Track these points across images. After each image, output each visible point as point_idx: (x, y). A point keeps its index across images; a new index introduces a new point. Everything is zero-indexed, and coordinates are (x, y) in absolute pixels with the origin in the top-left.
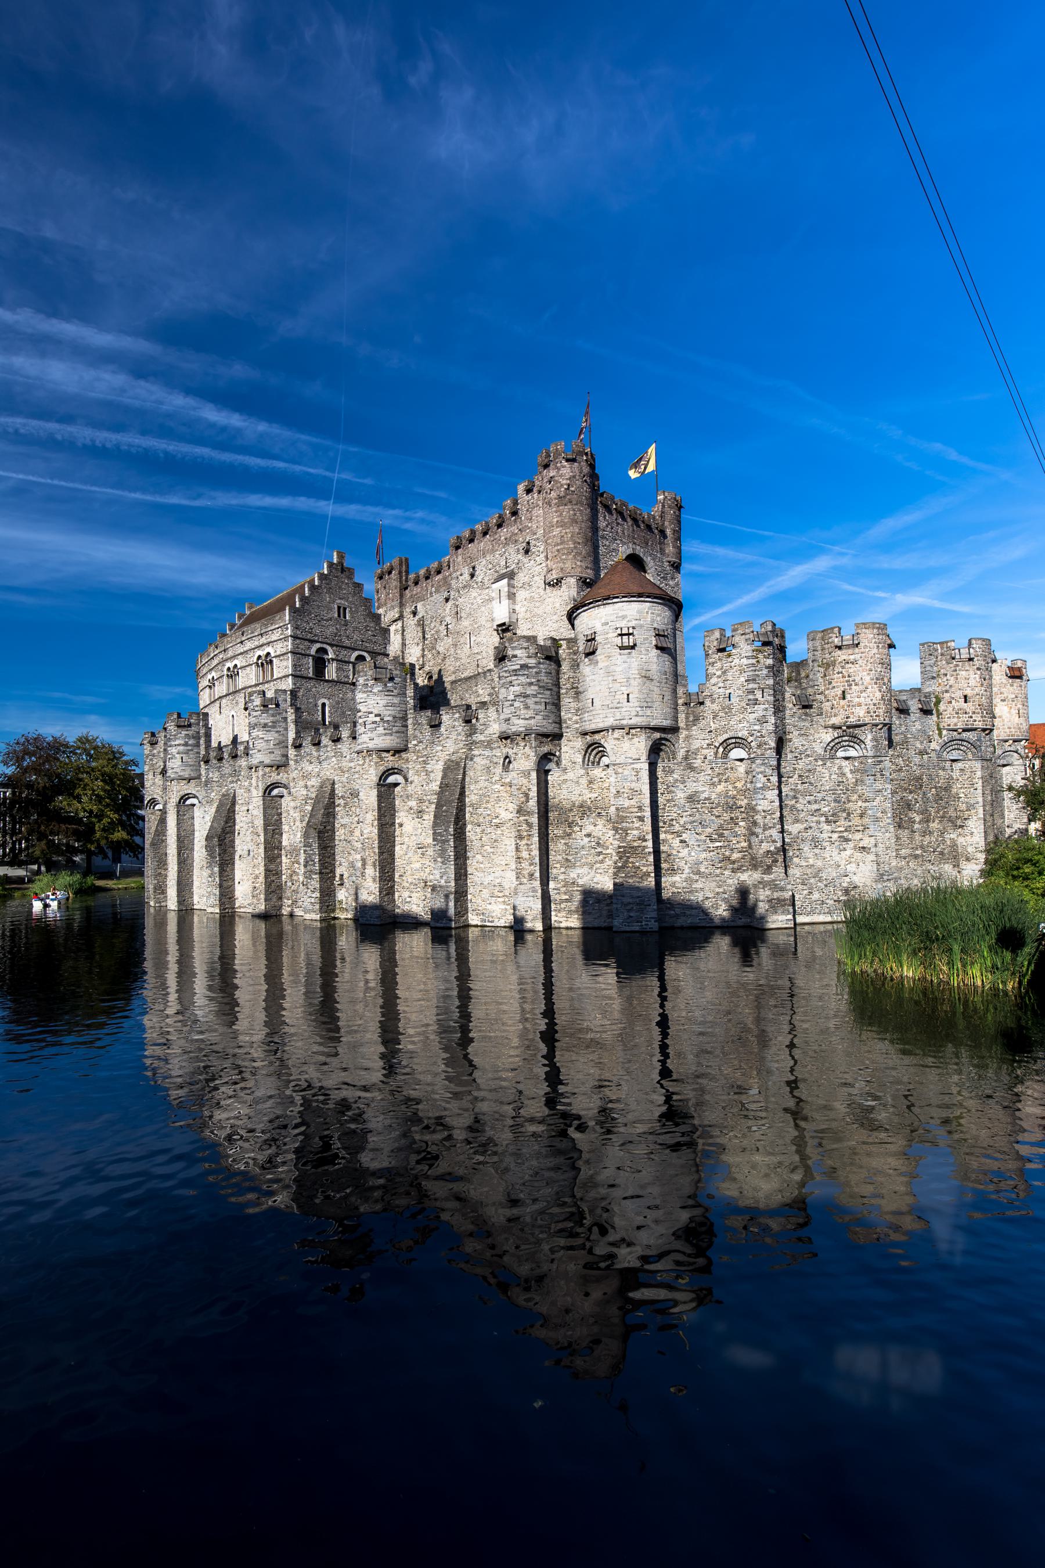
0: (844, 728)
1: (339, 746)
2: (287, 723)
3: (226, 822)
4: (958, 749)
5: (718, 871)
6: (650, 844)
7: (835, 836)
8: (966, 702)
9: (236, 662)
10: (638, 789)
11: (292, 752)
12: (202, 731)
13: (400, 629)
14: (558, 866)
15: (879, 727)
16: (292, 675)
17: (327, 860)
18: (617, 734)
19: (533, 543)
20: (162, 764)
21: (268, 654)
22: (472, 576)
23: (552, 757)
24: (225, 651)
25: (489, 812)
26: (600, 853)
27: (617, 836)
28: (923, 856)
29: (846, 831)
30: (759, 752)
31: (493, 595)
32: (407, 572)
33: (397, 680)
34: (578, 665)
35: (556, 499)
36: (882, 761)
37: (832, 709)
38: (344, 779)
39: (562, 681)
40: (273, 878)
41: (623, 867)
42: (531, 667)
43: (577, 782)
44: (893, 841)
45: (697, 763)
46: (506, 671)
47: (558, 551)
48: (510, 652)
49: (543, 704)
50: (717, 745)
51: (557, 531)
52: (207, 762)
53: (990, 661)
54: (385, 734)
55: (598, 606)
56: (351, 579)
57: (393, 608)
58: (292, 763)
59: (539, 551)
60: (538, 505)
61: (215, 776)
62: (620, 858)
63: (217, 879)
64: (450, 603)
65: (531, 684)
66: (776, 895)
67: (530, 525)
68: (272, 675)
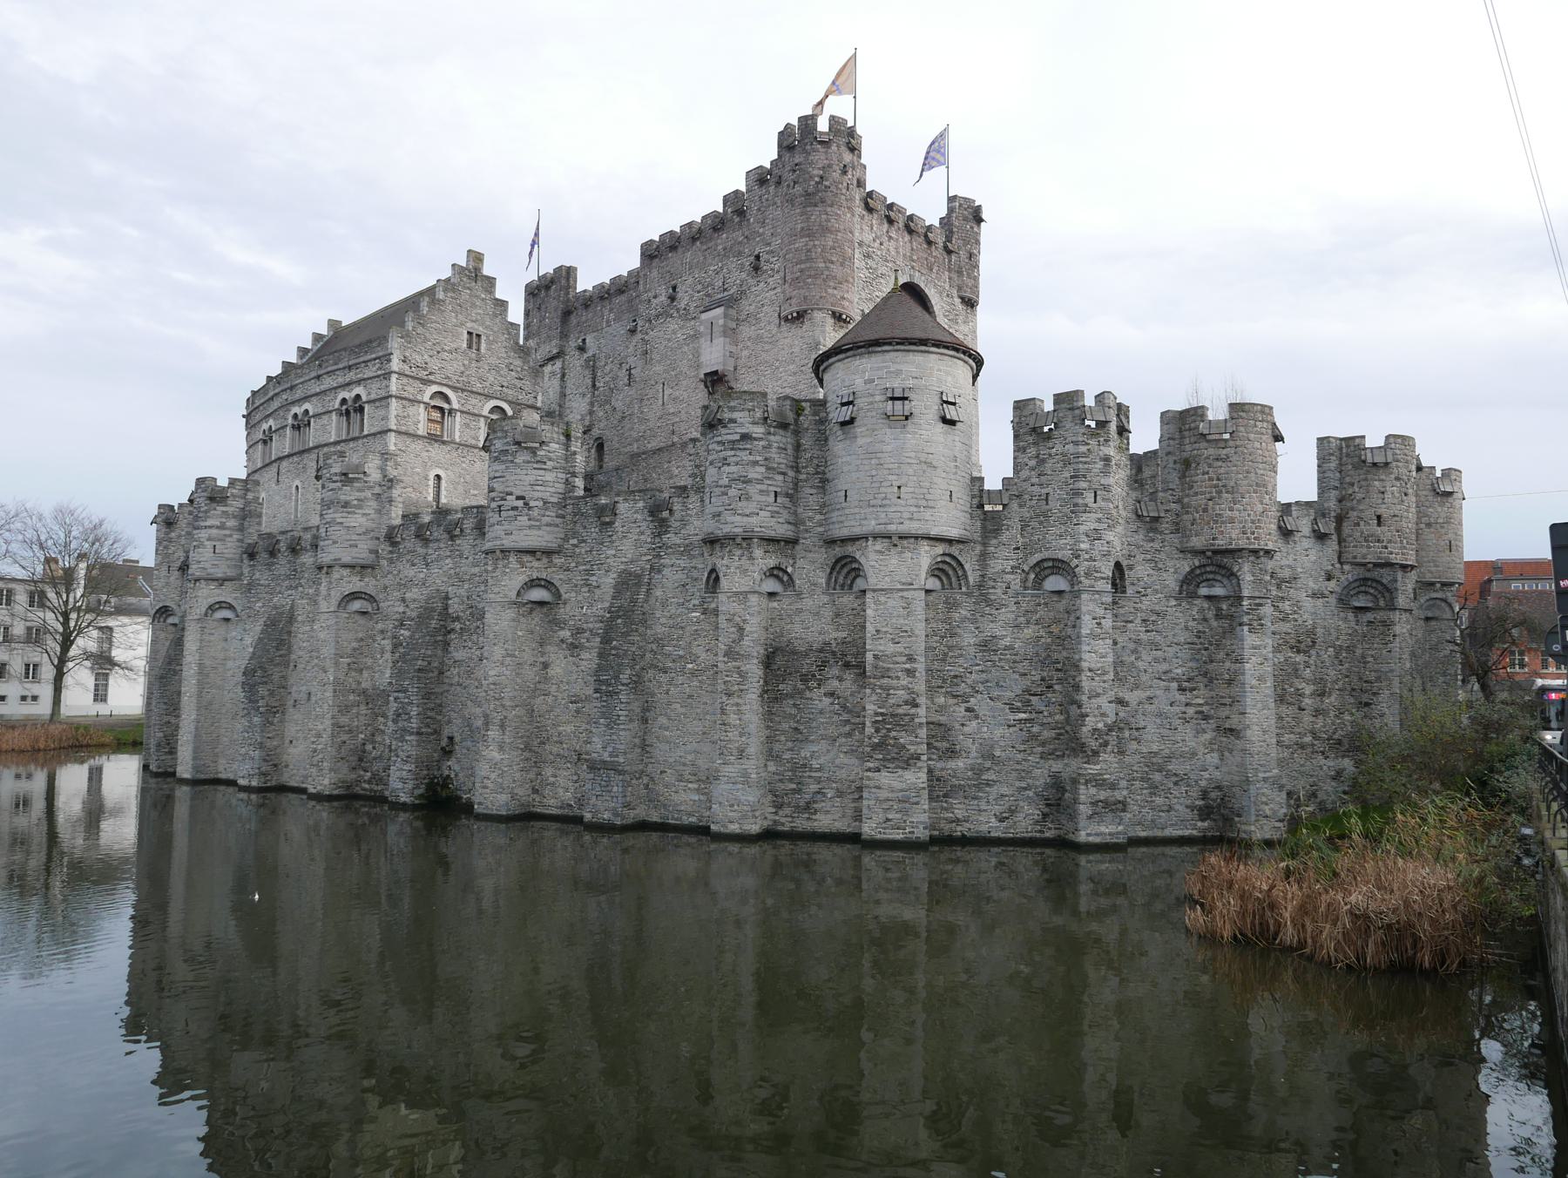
0: (1209, 554)
1: (458, 542)
4: (1366, 593)
5: (1020, 756)
6: (922, 711)
7: (1191, 711)
8: (1379, 524)
9: (307, 406)
10: (908, 628)
13: (558, 371)
14: (783, 738)
15: (1262, 553)
17: (429, 714)
18: (879, 545)
19: (764, 257)
20: (181, 554)
21: (358, 397)
22: (672, 299)
23: (781, 574)
24: (292, 388)
25: (681, 653)
26: (847, 722)
27: (874, 698)
28: (1313, 745)
29: (1207, 703)
30: (1086, 582)
31: (702, 329)
33: (554, 446)
34: (826, 440)
35: (803, 196)
36: (1261, 605)
37: (1193, 525)
38: (462, 592)
39: (802, 462)
40: (345, 737)
41: (878, 745)
42: (755, 439)
44: (1273, 722)
45: (997, 593)
46: (719, 443)
47: (801, 271)
48: (727, 415)
49: (773, 495)
50: (1026, 568)
53: (1414, 468)
54: (530, 527)
55: (861, 354)
57: (549, 339)
61: (262, 576)
62: (877, 731)
64: (639, 336)
65: (756, 463)
66: (1103, 795)
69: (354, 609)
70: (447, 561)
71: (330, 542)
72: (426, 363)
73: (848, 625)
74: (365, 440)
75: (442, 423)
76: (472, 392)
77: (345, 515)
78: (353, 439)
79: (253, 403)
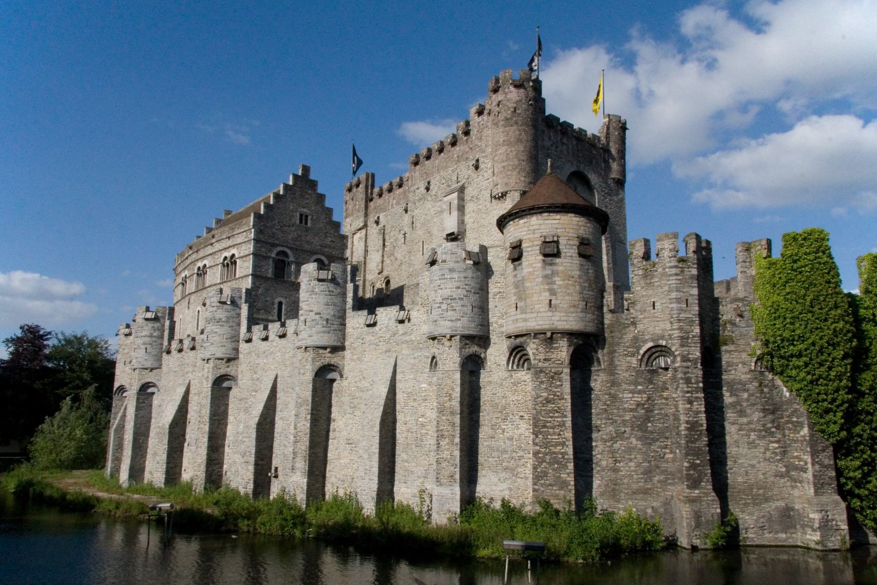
2: (240, 320)
9: (206, 262)
11: (243, 346)
12: (167, 323)
16: (252, 275)
21: (233, 255)
22: (428, 189)
24: (197, 252)
31: (444, 207)
32: (373, 186)
35: (503, 120)
38: (286, 373)
43: (502, 385)
47: (504, 167)
51: (502, 150)
54: (324, 332)
56: (315, 190)
58: (241, 356)
59: (487, 168)
60: (487, 127)
64: (409, 213)
65: (458, 288)
67: (479, 144)
68: (235, 276)
72: (273, 234)
73: (522, 391)
76: (302, 250)
77: (218, 327)
78: (230, 281)
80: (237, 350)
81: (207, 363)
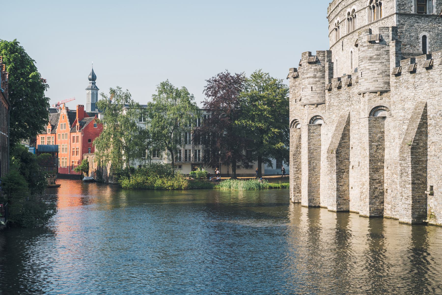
1: (431, 73)
3: (343, 138)
9: (354, 7)
12: (327, 66)
16: (396, 13)
52: (330, 90)
58: (392, 89)
63: (335, 184)
68: (381, 16)
69: (378, 116)
70: (426, 85)
71: (363, 80)
74: (383, 21)
75: (426, 5)
77: (371, 64)
78: (377, 22)
79: (330, 10)
80: (388, 83)
81: (363, 97)
